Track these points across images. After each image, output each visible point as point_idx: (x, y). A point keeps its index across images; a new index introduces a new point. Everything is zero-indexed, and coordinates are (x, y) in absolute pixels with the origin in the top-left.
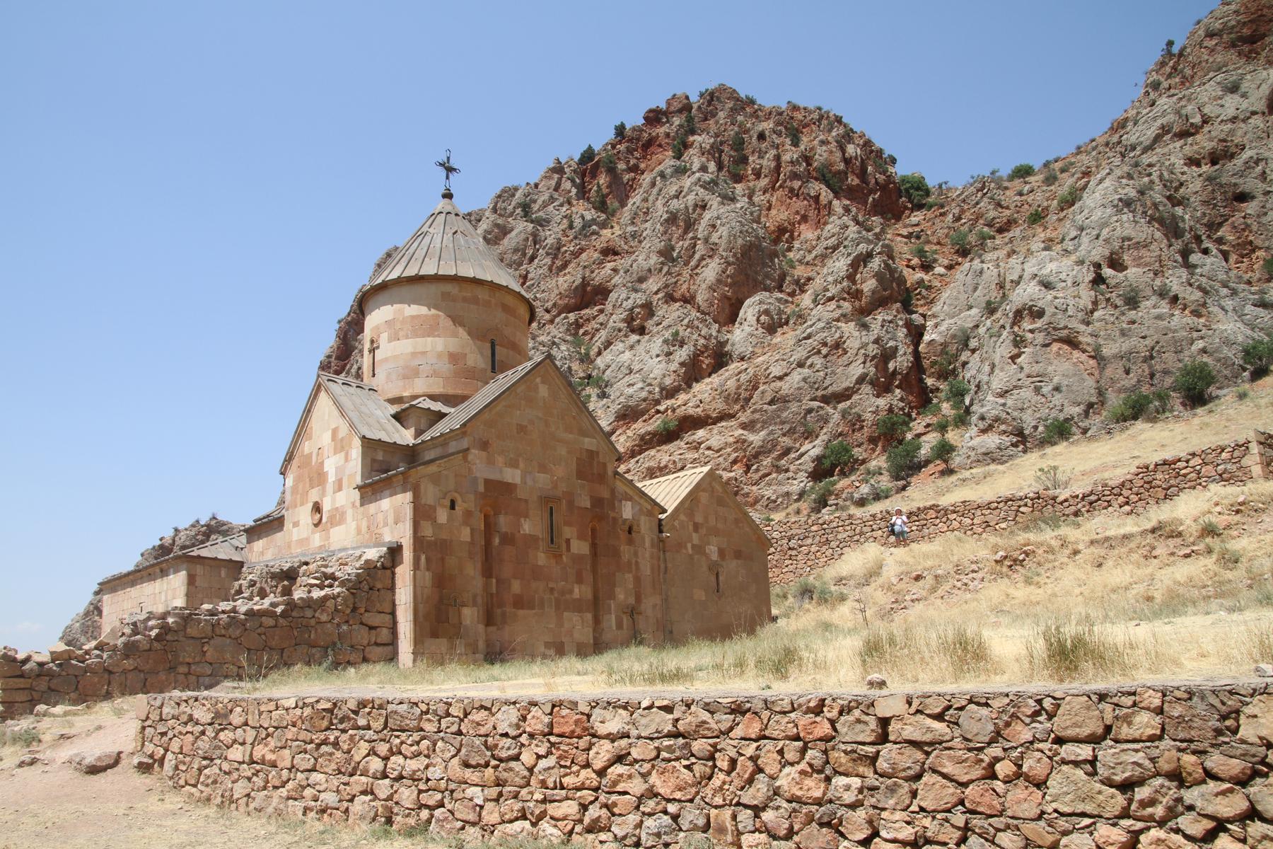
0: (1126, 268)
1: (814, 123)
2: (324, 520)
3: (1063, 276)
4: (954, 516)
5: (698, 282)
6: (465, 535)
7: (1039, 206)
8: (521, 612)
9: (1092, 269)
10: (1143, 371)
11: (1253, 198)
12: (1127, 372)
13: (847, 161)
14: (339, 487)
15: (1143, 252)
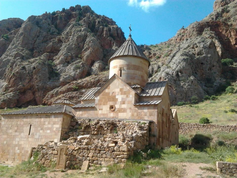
0: (183, 73)
1: (110, 22)
2: (116, 110)
3: (170, 72)
4: (215, 128)
5: (84, 54)
6: (161, 121)
7: (159, 55)
8: (164, 140)
9: (176, 72)
10: (184, 95)
11: (204, 64)
12: (181, 95)
13: (118, 34)
14: (123, 103)
15: (187, 71)
